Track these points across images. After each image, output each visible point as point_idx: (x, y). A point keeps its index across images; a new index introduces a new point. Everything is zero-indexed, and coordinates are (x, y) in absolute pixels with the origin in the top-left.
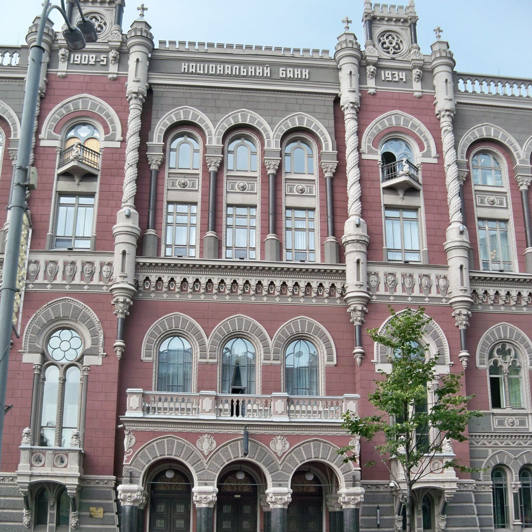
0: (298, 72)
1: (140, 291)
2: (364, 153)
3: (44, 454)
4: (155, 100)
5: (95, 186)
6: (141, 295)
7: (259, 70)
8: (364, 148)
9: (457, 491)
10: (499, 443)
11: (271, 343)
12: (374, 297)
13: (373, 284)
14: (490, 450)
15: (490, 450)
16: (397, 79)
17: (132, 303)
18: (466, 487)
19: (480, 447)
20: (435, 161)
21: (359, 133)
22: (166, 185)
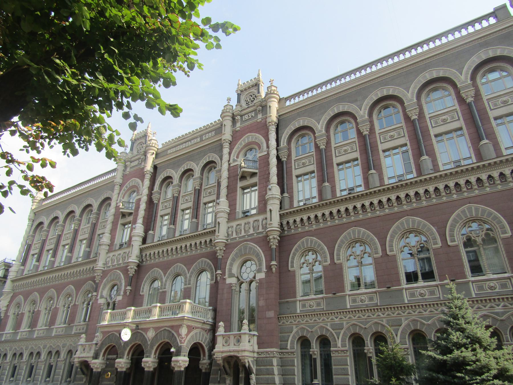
0: (210, 134)
1: (144, 261)
2: (231, 163)
3: (86, 346)
4: (158, 170)
5: (131, 218)
6: (144, 263)
7: (195, 140)
8: (231, 161)
9: (257, 358)
10: (317, 320)
11: (188, 275)
12: (229, 240)
13: (230, 233)
14: (294, 326)
15: (294, 326)
16: (250, 117)
17: (136, 268)
18: (269, 354)
19: (289, 325)
20: (266, 153)
21: (230, 154)
22: (160, 208)
